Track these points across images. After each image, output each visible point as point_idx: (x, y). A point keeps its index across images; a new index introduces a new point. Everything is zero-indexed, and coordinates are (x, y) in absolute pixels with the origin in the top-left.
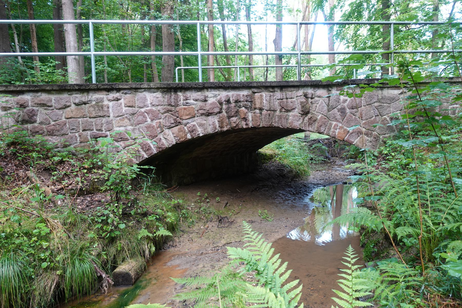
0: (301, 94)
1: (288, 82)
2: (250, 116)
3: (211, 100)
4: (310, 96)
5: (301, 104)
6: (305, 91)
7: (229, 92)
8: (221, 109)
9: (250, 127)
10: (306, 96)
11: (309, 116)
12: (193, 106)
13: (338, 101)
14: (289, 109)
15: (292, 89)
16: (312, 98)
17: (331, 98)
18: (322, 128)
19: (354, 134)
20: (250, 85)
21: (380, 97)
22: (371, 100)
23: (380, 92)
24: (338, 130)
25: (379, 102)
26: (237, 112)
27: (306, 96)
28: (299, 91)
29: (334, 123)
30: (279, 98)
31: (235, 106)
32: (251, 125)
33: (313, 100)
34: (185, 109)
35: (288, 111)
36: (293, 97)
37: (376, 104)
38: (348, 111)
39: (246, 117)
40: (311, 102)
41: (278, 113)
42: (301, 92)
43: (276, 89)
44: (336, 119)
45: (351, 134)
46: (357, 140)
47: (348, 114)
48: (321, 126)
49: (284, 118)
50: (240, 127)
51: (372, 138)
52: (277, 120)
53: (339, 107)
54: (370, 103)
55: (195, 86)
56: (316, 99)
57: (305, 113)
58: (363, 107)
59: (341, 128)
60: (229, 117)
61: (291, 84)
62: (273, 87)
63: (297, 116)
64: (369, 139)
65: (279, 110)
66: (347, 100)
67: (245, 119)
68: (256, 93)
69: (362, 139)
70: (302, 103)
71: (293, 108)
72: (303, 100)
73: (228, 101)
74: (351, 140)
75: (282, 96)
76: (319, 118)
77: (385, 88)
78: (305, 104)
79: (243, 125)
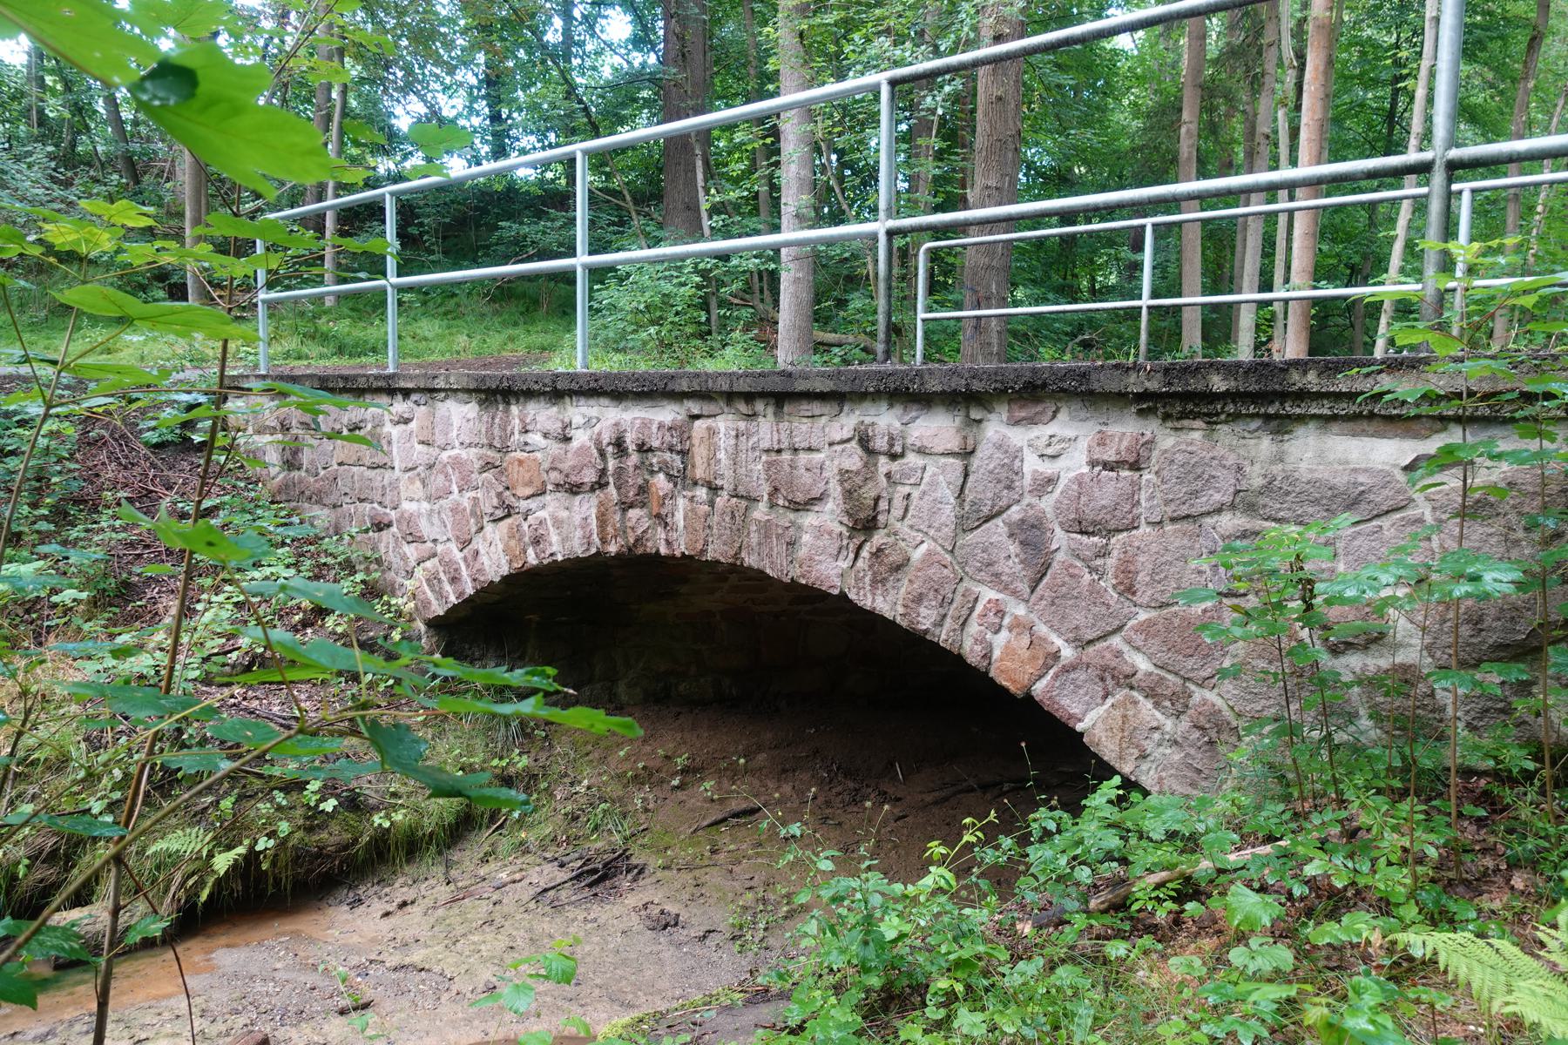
0: (846, 434)
1: (790, 375)
2: (680, 510)
3: (581, 438)
4: (880, 443)
5: (841, 482)
6: (868, 420)
7: (626, 409)
8: (603, 472)
9: (678, 554)
10: (864, 441)
11: (878, 538)
12: (538, 455)
13: (1008, 477)
14: (800, 497)
15: (816, 407)
16: (894, 457)
17: (975, 462)
18: (923, 611)
19: (1080, 675)
20: (670, 387)
21: (1258, 482)
22: (1195, 494)
23: (1265, 445)
24: (1004, 634)
25: (1251, 508)
26: (643, 489)
27: (864, 441)
28: (843, 419)
29: (988, 594)
30: (765, 444)
31: (636, 467)
32: (681, 548)
33: (895, 466)
34: (521, 462)
35: (798, 507)
36: (814, 445)
37: (1229, 522)
38: (1060, 539)
39: (663, 511)
40: (888, 475)
41: (760, 512)
42: (847, 422)
43: (759, 406)
44: (997, 575)
45: (1067, 669)
46: (1101, 710)
47: (1060, 556)
48: (919, 599)
49: (778, 536)
50: (650, 547)
51: (1185, 723)
52: (754, 539)
53: (1015, 513)
54: (1184, 510)
55: (536, 387)
56: (912, 459)
57: (864, 524)
58: (1145, 528)
59: (1018, 626)
60: (626, 506)
61: (801, 386)
62: (749, 397)
63: (830, 533)
64: (1169, 725)
65: (766, 497)
66: (1051, 481)
67: (662, 519)
68: (697, 417)
69: (1117, 713)
70: (844, 474)
71: (816, 493)
72: (853, 459)
73: (619, 444)
74: (1065, 702)
75: (776, 437)
76: (917, 555)
77: (1301, 419)
78: (858, 480)
79: (659, 543)
